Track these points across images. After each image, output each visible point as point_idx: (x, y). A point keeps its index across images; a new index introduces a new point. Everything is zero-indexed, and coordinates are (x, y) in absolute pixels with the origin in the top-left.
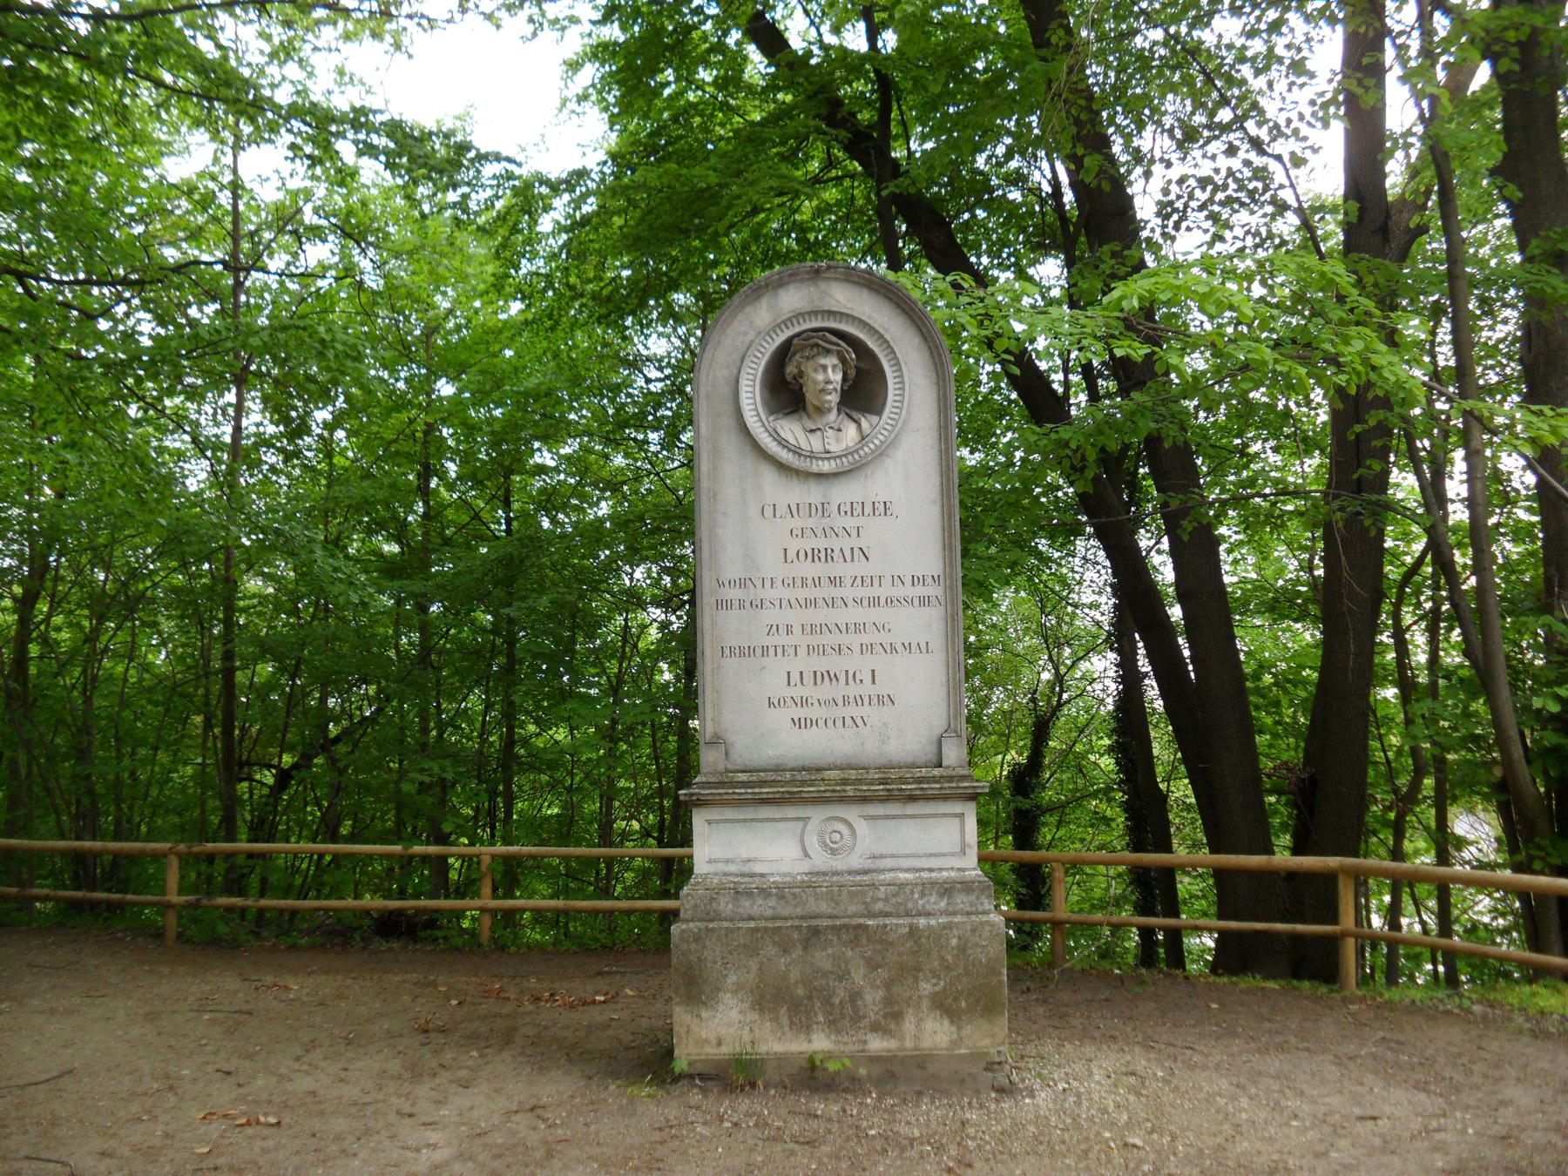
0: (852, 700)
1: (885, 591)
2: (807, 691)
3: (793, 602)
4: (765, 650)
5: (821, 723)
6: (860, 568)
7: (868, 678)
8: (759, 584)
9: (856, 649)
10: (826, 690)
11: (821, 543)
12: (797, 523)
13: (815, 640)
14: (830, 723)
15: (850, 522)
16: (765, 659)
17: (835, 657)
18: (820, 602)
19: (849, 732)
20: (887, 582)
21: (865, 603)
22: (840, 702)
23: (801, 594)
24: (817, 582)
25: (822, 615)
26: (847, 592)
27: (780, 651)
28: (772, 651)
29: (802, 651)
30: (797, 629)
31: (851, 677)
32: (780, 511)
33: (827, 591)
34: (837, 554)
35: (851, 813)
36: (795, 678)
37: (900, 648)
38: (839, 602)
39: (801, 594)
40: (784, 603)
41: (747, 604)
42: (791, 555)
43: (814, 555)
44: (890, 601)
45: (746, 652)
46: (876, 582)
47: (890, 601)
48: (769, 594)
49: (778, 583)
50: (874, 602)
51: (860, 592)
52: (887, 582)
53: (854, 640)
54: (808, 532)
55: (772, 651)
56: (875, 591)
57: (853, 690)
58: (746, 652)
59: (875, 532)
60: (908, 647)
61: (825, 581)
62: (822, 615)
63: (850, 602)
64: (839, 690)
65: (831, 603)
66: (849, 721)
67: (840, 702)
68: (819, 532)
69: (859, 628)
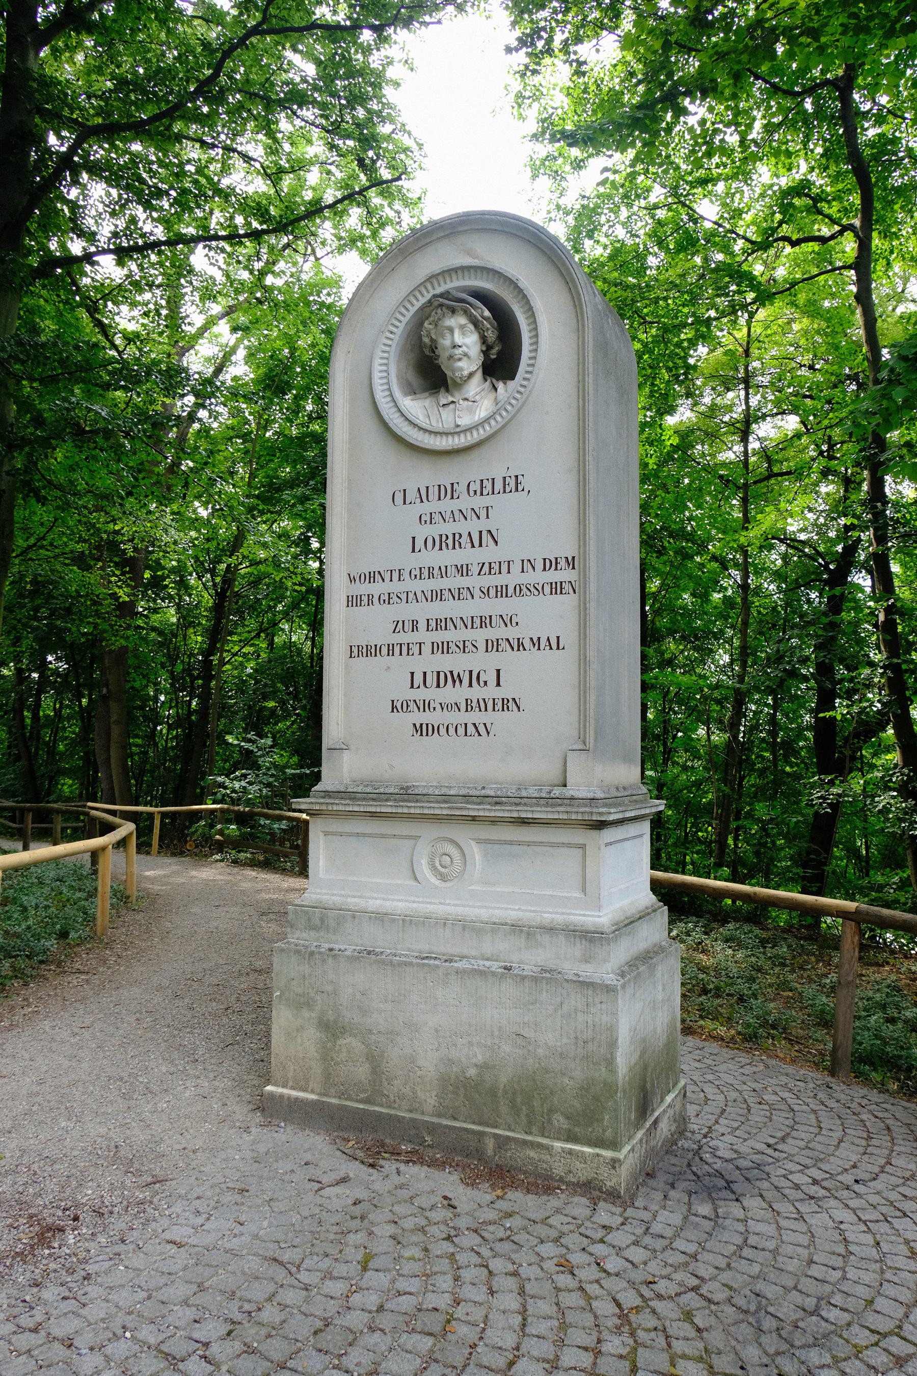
0: (474, 704)
1: (512, 579)
2: (430, 694)
3: (419, 594)
5: (443, 731)
6: (489, 553)
7: (492, 681)
8: (387, 577)
9: (481, 646)
10: (450, 693)
11: (448, 528)
12: (426, 508)
13: (440, 636)
14: (452, 730)
15: (478, 502)
18: (446, 594)
20: (516, 567)
21: (492, 592)
23: (429, 585)
24: (444, 572)
26: (474, 582)
27: (405, 648)
28: (397, 649)
29: (427, 649)
30: (422, 625)
31: (474, 678)
32: (412, 495)
33: (455, 582)
35: (465, 835)
36: (419, 679)
37: (527, 644)
38: (465, 593)
39: (429, 585)
40: (411, 595)
41: (376, 600)
42: (419, 544)
43: (441, 542)
44: (519, 590)
46: (504, 568)
47: (519, 590)
49: (406, 575)
50: (502, 592)
52: (516, 567)
53: (480, 636)
54: (437, 517)
55: (397, 649)
57: (477, 693)
59: (506, 512)
60: (536, 643)
61: (452, 571)
63: (477, 593)
64: (459, 694)
65: (456, 594)
66: (471, 729)
67: (463, 708)
68: (448, 516)
69: (485, 622)
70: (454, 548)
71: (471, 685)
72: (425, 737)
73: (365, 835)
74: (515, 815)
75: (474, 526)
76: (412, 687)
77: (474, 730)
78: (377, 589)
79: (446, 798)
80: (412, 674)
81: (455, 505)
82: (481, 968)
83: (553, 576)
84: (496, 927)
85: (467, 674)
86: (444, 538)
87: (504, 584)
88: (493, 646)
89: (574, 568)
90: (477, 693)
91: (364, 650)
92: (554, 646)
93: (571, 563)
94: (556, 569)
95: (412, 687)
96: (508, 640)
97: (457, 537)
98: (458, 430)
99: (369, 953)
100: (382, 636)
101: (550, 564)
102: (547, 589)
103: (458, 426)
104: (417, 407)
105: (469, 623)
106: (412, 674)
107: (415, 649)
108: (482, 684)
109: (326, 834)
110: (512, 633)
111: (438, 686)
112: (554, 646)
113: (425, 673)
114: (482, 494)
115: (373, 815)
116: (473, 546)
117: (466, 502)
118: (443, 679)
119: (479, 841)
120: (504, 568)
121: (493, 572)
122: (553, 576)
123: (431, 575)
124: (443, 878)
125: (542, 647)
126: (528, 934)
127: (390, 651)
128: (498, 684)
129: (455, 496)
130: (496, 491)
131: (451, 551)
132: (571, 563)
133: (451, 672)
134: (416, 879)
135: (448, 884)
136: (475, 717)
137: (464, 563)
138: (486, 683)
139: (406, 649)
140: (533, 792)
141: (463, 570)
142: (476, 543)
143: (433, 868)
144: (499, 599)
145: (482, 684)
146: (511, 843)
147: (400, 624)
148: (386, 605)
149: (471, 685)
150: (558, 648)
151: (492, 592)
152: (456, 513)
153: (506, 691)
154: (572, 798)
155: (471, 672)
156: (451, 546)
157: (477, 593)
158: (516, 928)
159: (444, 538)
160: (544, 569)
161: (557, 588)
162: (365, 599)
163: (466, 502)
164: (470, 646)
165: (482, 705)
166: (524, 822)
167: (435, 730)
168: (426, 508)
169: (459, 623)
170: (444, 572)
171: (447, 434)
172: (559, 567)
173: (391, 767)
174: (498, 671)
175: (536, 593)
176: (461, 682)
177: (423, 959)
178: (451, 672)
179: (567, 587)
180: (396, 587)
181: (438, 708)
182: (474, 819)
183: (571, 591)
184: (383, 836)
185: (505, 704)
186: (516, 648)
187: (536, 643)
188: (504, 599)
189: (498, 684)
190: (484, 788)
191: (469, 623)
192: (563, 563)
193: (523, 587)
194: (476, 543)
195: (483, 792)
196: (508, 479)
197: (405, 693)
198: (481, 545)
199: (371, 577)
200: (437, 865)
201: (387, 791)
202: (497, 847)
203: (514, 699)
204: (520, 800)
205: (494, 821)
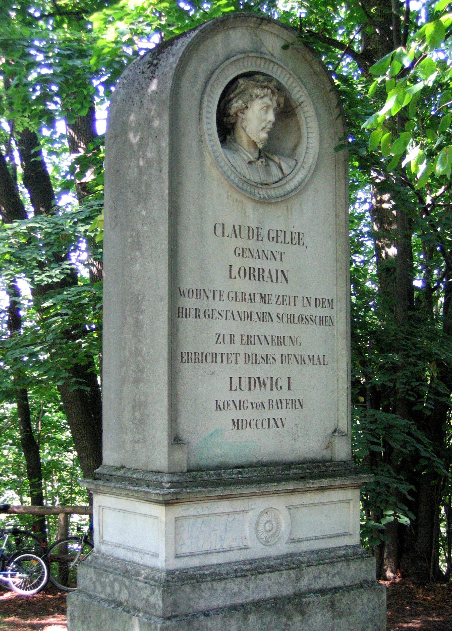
3: (235, 314)
4: (214, 356)
5: (253, 424)
7: (285, 387)
8: (210, 295)
9: (278, 358)
11: (256, 264)
12: (240, 243)
14: (259, 424)
15: (277, 247)
16: (214, 364)
17: (264, 366)
18: (255, 317)
19: (273, 431)
20: (299, 301)
22: (267, 405)
23: (243, 307)
25: (255, 328)
29: (241, 359)
30: (237, 339)
31: (274, 384)
32: (229, 230)
34: (266, 274)
38: (267, 316)
39: (243, 307)
40: (229, 314)
41: (202, 313)
45: (199, 358)
48: (219, 305)
49: (225, 296)
50: (291, 319)
51: (281, 309)
52: (299, 301)
53: (277, 351)
54: (247, 253)
56: (290, 310)
57: (275, 395)
58: (199, 358)
60: (311, 359)
62: (255, 328)
63: (275, 318)
65: (262, 318)
66: (272, 422)
67: (267, 405)
68: (255, 253)
69: (280, 341)
70: (259, 280)
71: (272, 389)
72: (240, 430)
77: (274, 424)
85: (269, 379)
87: (292, 313)
88: (285, 359)
91: (193, 357)
101: (319, 303)
107: (233, 358)
108: (279, 388)
111: (250, 389)
113: (240, 378)
114: (277, 242)
116: (272, 281)
123: (243, 299)
125: (315, 362)
129: (260, 238)
130: (287, 242)
133: (259, 378)
136: (275, 413)
137: (267, 293)
138: (281, 387)
139: (226, 358)
142: (274, 280)
147: (221, 336)
149: (272, 389)
150: (324, 364)
151: (285, 319)
152: (261, 253)
153: (294, 395)
161: (323, 320)
164: (271, 358)
165: (280, 404)
176: (265, 386)
181: (250, 407)
186: (300, 362)
188: (292, 324)
192: (326, 303)
193: (304, 318)
194: (274, 280)
197: (225, 395)
198: (277, 281)
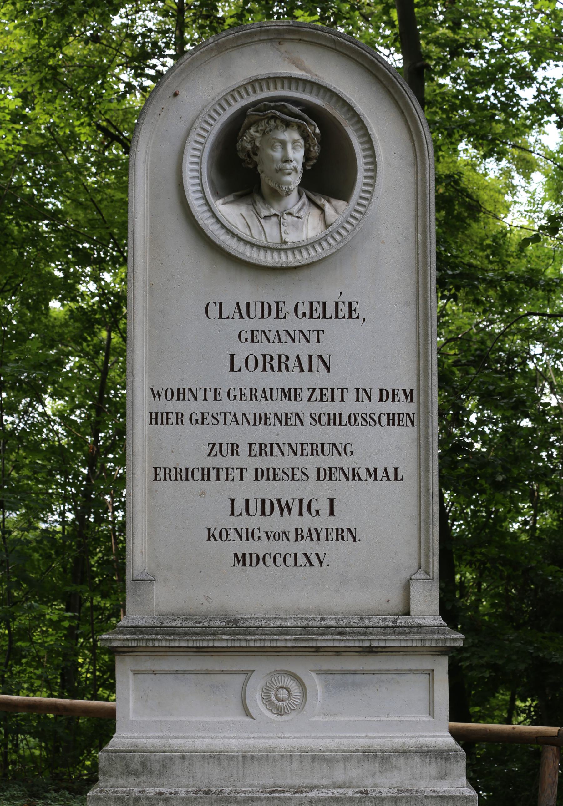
0: (305, 534)
1: (347, 408)
2: (255, 522)
3: (240, 417)
5: (269, 561)
6: (319, 379)
7: (325, 510)
8: (200, 395)
9: (313, 474)
10: (276, 522)
12: (247, 325)
13: (265, 462)
14: (280, 561)
20: (350, 396)
21: (324, 420)
23: (251, 407)
24: (268, 395)
26: (303, 407)
27: (223, 474)
28: (213, 474)
29: (249, 475)
30: (244, 450)
31: (305, 507)
35: (303, 667)
36: (240, 506)
37: (363, 473)
39: (251, 407)
41: (186, 419)
42: (239, 362)
44: (353, 419)
46: (338, 395)
47: (353, 419)
50: (334, 419)
52: (350, 396)
53: (311, 463)
54: (259, 336)
55: (213, 474)
56: (334, 407)
57: (307, 522)
59: (337, 336)
60: (373, 473)
63: (307, 420)
65: (285, 419)
66: (301, 559)
67: (292, 536)
68: (272, 336)
69: (316, 450)
73: (184, 672)
74: (367, 644)
75: (303, 349)
76: (232, 514)
78: (187, 407)
79: (283, 631)
80: (233, 501)
81: (281, 325)
82: (337, 795)
83: (390, 407)
84: (348, 756)
85: (297, 502)
86: (268, 359)
89: (412, 401)
90: (307, 522)
91: (173, 473)
92: (392, 477)
93: (408, 395)
94: (393, 400)
95: (232, 514)
96: (342, 469)
97: (284, 359)
98: (285, 247)
99: (206, 793)
100: (197, 459)
101: (386, 395)
102: (384, 420)
103: (286, 243)
104: (232, 213)
105: (300, 450)
106: (233, 501)
107: (237, 475)
108: (314, 513)
109: (136, 673)
110: (347, 462)
111: (263, 513)
112: (392, 477)
113: (247, 501)
115: (199, 651)
116: (302, 370)
117: (293, 324)
118: (266, 507)
119: (319, 673)
120: (338, 395)
121: (325, 398)
122: (390, 407)
124: (280, 712)
125: (379, 478)
126: (383, 758)
127: (205, 475)
128: (332, 513)
129: (281, 315)
131: (276, 374)
132: (408, 395)
133: (279, 501)
134: (248, 714)
135: (285, 718)
137: (292, 387)
140: (376, 621)
141: (289, 394)
142: (306, 367)
143: (268, 702)
144: (332, 428)
145: (314, 513)
146: (355, 672)
148: (199, 426)
149: (301, 514)
150: (396, 479)
151: (324, 420)
152: (283, 335)
153: (341, 521)
154: (420, 626)
155: (301, 501)
156: (276, 368)
157: (307, 420)
158: (368, 754)
159: (268, 359)
160: (381, 400)
161: (394, 420)
162: (173, 418)
163: (293, 324)
164: (300, 474)
165: (315, 535)
166: (371, 651)
167: (261, 559)
168: (247, 325)
169: (286, 449)
170: (268, 395)
171: (272, 249)
172: (397, 399)
173: (209, 599)
174: (332, 501)
175: (372, 423)
176: (290, 510)
177: (271, 792)
178: (279, 501)
179: (404, 419)
180: (211, 406)
181: (264, 537)
182: (317, 650)
183: (409, 423)
184: (208, 672)
185: (339, 534)
186: (351, 477)
187: (373, 473)
188: (338, 427)
189: (332, 513)
190: (323, 619)
191: (300, 450)
192: (401, 395)
194: (306, 367)
195: (324, 623)
196: (340, 305)
198: (311, 370)
199: (181, 394)
200: (273, 699)
201: (212, 624)
202: (338, 677)
203: (349, 530)
204: (365, 630)
205: (338, 652)
